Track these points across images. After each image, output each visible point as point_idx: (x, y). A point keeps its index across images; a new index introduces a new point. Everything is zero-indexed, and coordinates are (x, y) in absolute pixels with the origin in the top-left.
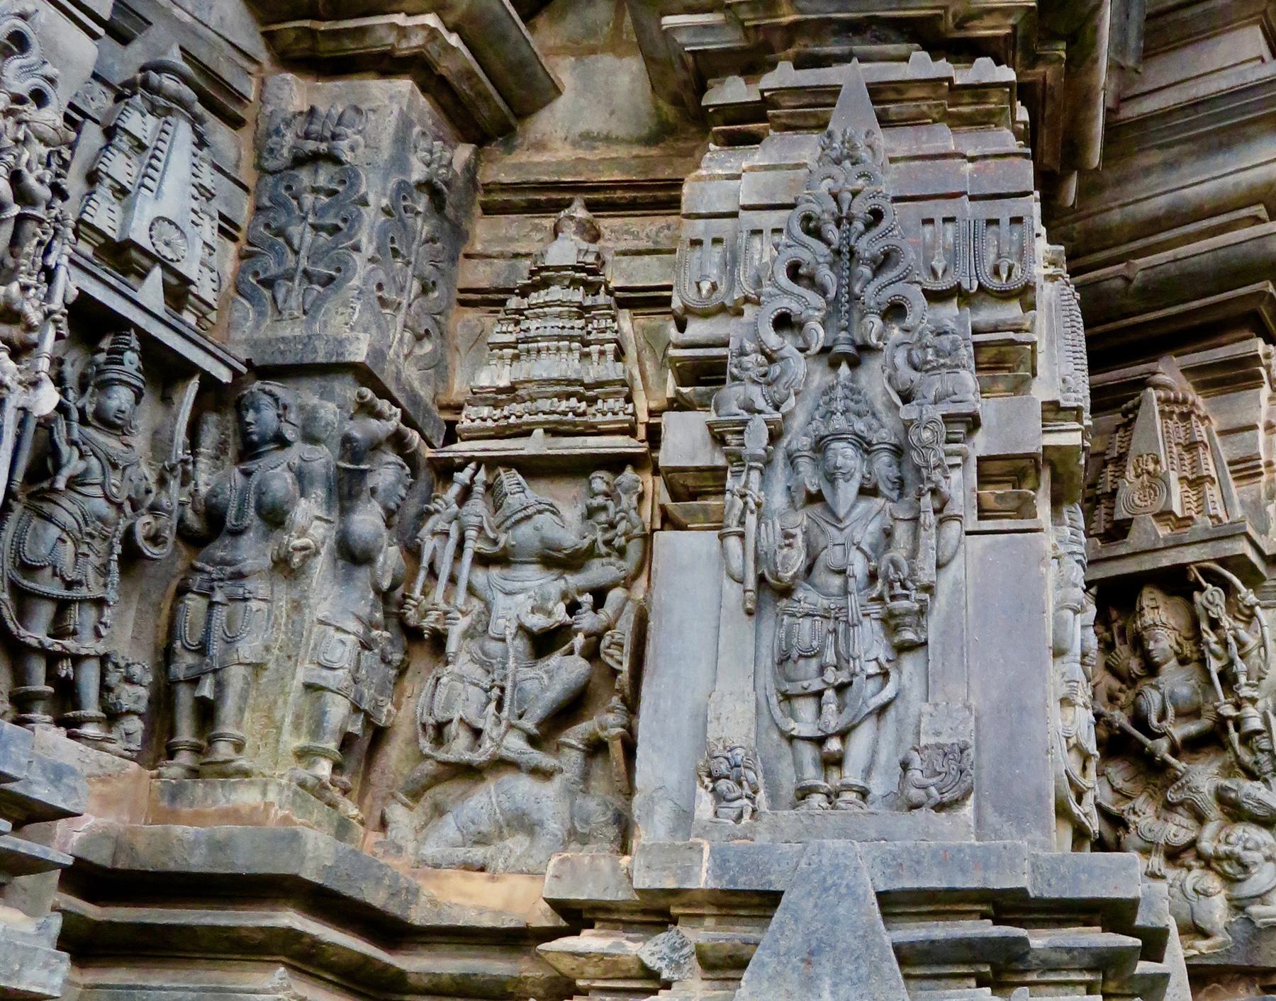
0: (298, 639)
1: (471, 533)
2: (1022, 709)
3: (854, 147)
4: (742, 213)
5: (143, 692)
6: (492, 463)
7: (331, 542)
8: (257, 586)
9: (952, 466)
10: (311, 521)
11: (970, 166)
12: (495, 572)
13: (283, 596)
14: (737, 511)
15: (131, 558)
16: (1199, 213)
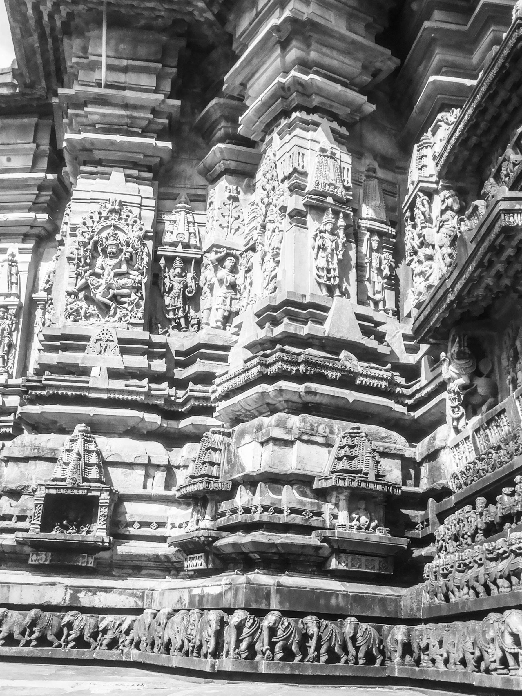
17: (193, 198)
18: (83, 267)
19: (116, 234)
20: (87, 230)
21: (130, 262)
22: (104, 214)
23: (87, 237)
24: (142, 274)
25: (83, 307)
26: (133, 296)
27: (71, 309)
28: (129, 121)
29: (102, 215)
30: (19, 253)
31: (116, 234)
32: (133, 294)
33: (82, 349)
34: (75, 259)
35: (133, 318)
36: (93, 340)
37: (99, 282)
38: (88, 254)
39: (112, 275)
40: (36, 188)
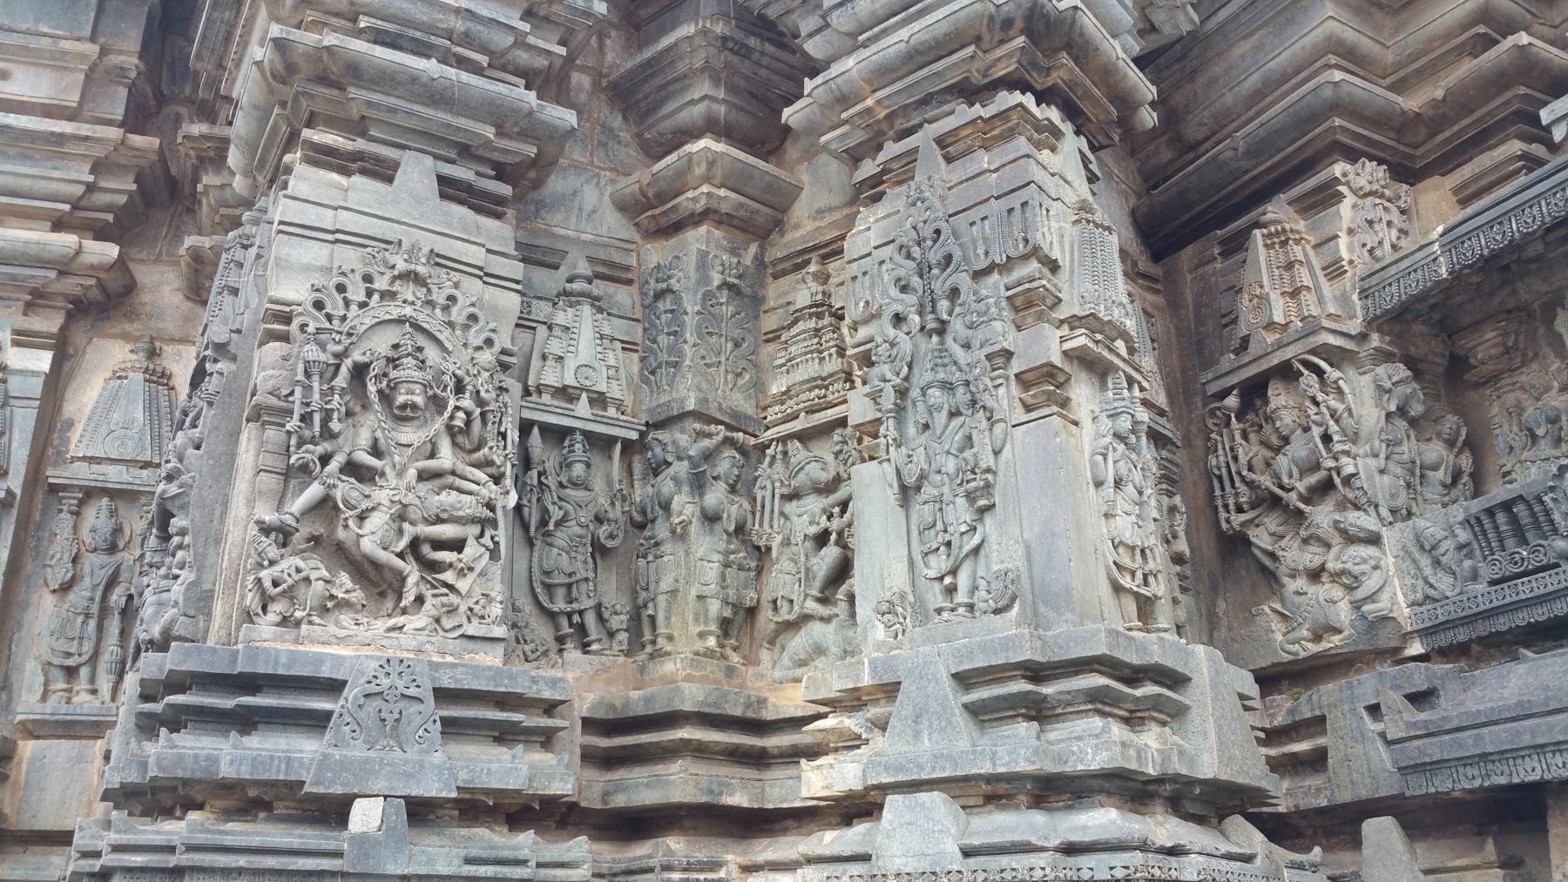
0: (694, 570)
1: (777, 484)
2: (1053, 535)
3: (922, 192)
4: (875, 252)
5: (624, 617)
6: (783, 440)
7: (698, 513)
8: (667, 548)
9: (996, 387)
10: (684, 506)
11: (995, 175)
12: (794, 503)
13: (680, 549)
14: (883, 447)
15: (600, 550)
16: (1285, 77)
17: (601, 269)
18: (313, 441)
19: (420, 349)
20: (327, 325)
21: (460, 439)
22: (381, 284)
23: (332, 348)
24: (497, 479)
25: (314, 575)
26: (471, 550)
27: (275, 584)
28: (460, 25)
29: (376, 286)
30: (16, 343)
31: (420, 349)
32: (471, 541)
33: (317, 722)
34: (291, 412)
35: (475, 621)
36: (350, 693)
37: (367, 497)
38: (334, 405)
39: (412, 473)
40: (87, 167)
